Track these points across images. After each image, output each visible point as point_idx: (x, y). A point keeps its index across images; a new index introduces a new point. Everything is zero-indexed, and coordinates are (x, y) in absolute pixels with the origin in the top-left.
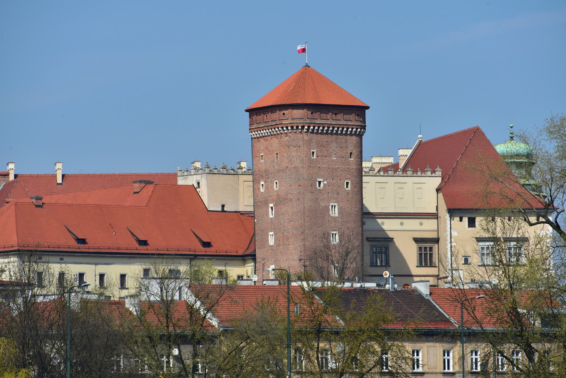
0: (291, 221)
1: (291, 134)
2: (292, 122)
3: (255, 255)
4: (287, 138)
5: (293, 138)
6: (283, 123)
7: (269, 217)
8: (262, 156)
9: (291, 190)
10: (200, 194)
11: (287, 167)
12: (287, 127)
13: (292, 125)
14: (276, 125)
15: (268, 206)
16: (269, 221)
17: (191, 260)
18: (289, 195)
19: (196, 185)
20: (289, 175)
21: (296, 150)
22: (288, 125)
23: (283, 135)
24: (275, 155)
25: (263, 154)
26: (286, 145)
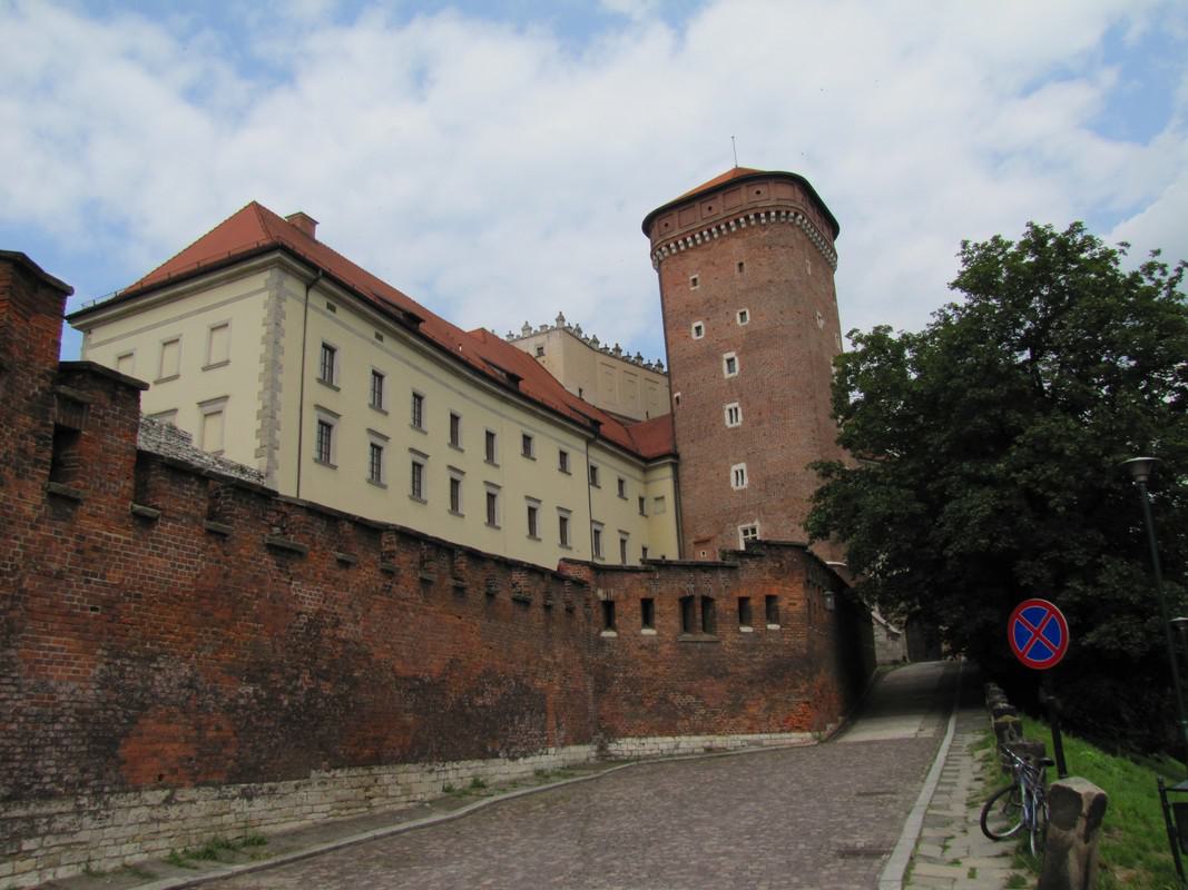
3: (676, 456)
4: (767, 233)
7: (723, 378)
8: (695, 280)
10: (545, 366)
11: (770, 281)
12: (768, 214)
13: (779, 209)
14: (741, 212)
15: (719, 359)
16: (726, 384)
17: (589, 442)
18: (780, 328)
19: (534, 353)
21: (787, 252)
22: (770, 209)
24: (736, 268)
25: (696, 276)
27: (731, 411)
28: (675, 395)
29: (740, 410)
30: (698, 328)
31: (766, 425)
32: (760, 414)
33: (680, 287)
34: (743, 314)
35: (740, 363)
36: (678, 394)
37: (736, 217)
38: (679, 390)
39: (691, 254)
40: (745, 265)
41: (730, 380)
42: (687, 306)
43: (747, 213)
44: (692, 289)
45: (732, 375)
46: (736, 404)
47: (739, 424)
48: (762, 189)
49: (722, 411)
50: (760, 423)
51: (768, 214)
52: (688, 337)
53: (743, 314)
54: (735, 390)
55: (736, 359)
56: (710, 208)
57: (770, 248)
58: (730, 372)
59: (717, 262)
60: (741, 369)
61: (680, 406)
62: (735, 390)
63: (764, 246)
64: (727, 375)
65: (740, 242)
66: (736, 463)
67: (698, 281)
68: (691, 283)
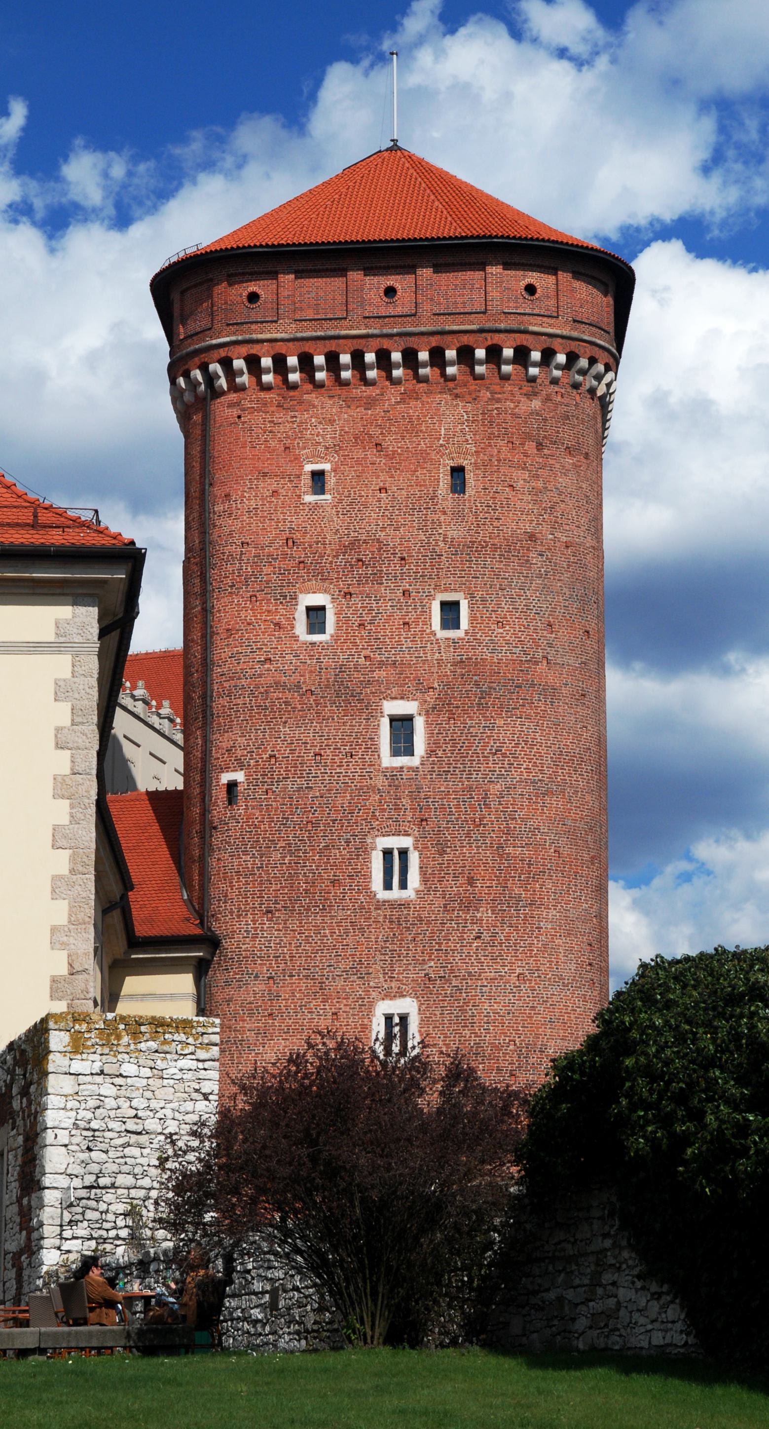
0: (549, 792)
1: (556, 389)
2: (575, 334)
3: (213, 943)
4: (536, 404)
5: (561, 409)
6: (532, 328)
8: (318, 476)
9: (550, 645)
11: (532, 537)
12: (548, 355)
13: (574, 346)
14: (481, 331)
15: (372, 713)
16: (380, 782)
20: (540, 576)
21: (576, 466)
22: (556, 344)
23: (508, 387)
24: (445, 481)
25: (327, 467)
26: (528, 436)
27: (387, 853)
28: (225, 778)
29: (414, 859)
30: (316, 614)
31: (485, 914)
32: (471, 881)
33: (272, 484)
34: (450, 609)
35: (430, 734)
36: (239, 776)
37: (465, 340)
38: (241, 766)
39: (312, 397)
40: (470, 476)
41: (393, 775)
42: (290, 541)
43: (497, 339)
44: (309, 498)
45: (402, 761)
46: (406, 842)
47: (409, 894)
48: (542, 281)
49: (364, 851)
50: (469, 904)
51: (548, 355)
52: (282, 627)
53: (450, 609)
54: (406, 802)
55: (419, 724)
56: (390, 292)
57: (540, 446)
58: (395, 753)
59: (391, 443)
60: (431, 752)
61: (240, 809)
62: (406, 802)
63: (528, 436)
64: (387, 760)
65: (462, 409)
66: (389, 995)
67: (331, 481)
68: (306, 480)
